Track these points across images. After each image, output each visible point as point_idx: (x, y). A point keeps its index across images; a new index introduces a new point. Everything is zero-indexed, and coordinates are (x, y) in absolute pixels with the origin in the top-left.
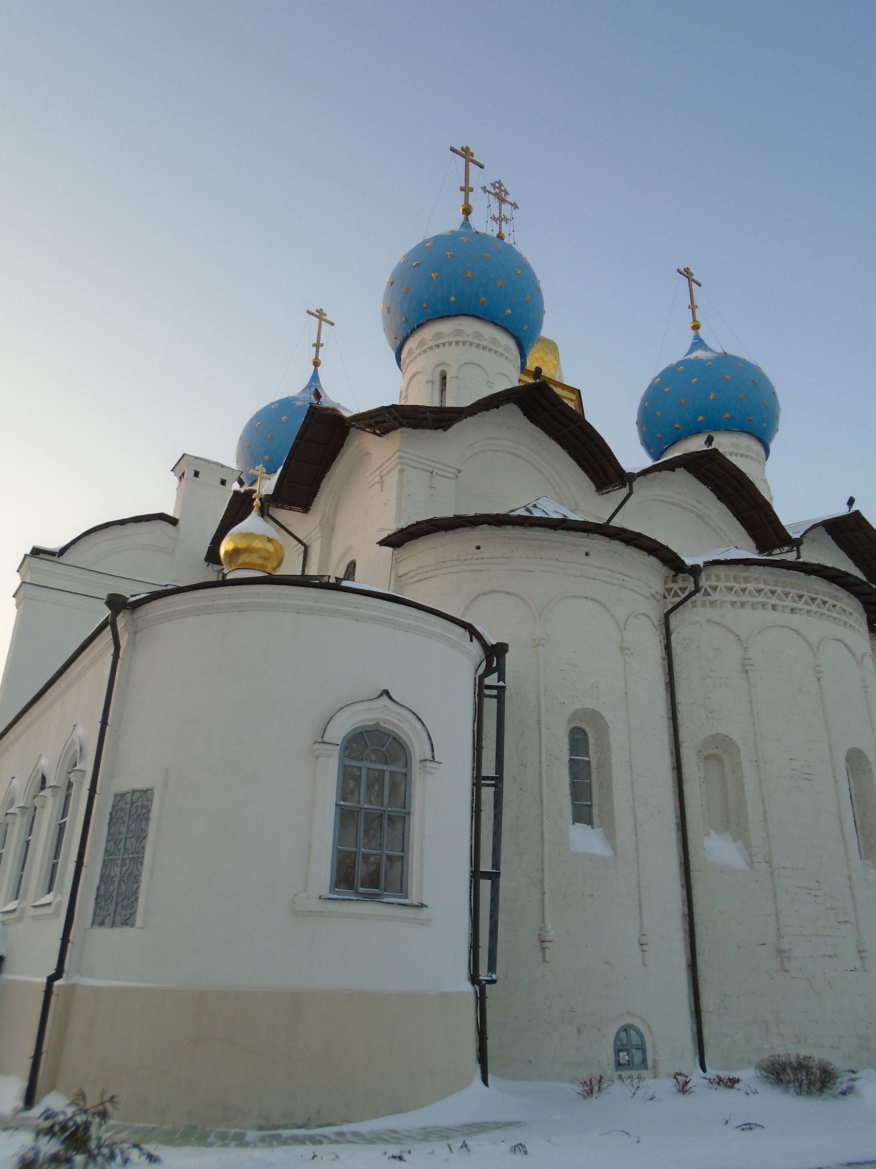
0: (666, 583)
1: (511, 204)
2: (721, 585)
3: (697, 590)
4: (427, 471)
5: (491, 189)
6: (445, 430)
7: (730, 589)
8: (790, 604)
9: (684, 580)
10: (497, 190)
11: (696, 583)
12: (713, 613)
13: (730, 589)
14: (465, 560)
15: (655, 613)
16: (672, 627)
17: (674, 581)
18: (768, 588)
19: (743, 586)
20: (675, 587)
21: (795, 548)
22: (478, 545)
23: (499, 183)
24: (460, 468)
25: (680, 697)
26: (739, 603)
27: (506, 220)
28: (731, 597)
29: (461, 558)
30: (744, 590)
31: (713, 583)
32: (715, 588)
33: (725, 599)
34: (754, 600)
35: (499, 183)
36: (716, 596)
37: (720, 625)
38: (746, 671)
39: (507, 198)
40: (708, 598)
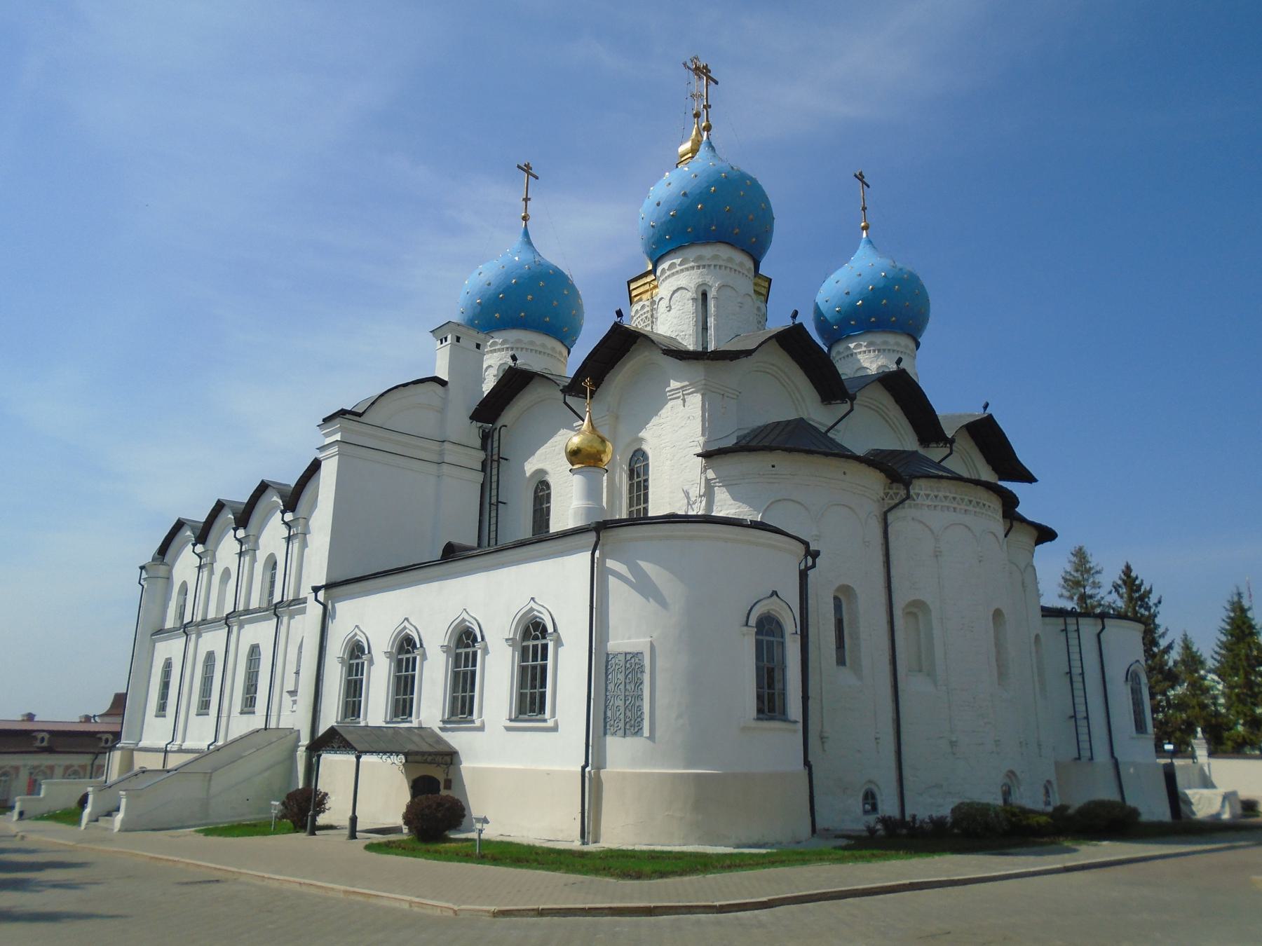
0: (885, 489)
2: (922, 493)
3: (908, 497)
4: (720, 394)
8: (964, 507)
9: (897, 489)
11: (908, 492)
13: (928, 496)
14: (763, 475)
16: (889, 521)
17: (889, 488)
18: (951, 495)
19: (936, 493)
20: (891, 492)
21: (948, 445)
22: (773, 464)
26: (933, 506)
28: (928, 502)
29: (761, 473)
31: (917, 491)
32: (918, 495)
33: (924, 503)
34: (943, 504)
36: (919, 501)
37: (921, 522)
38: (937, 556)
40: (915, 502)
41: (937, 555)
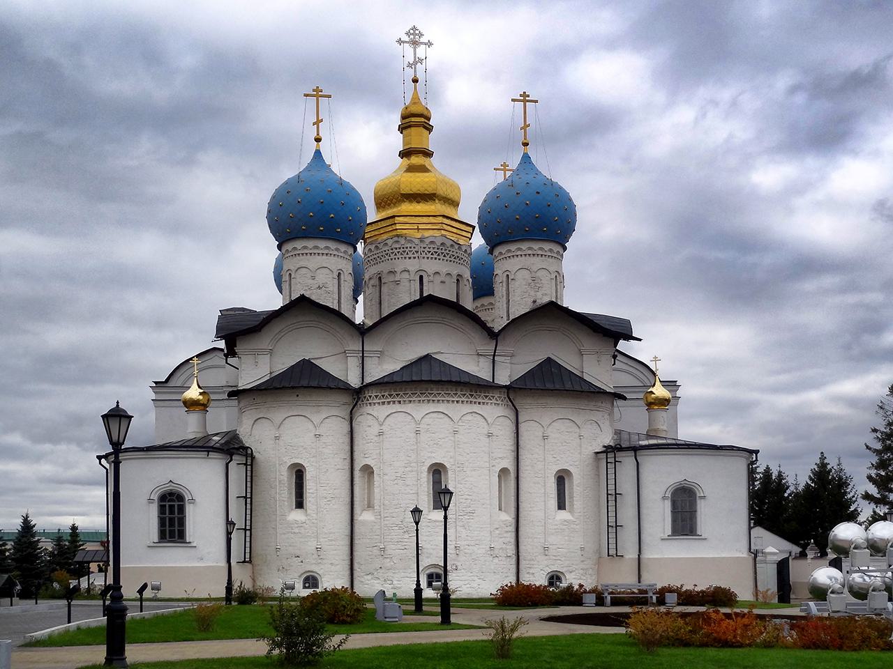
1: (426, 44)
5: (407, 39)
6: (260, 331)
7: (376, 396)
10: (412, 37)
12: (369, 409)
13: (376, 396)
15: (346, 414)
23: (414, 28)
24: (271, 348)
25: (356, 448)
27: (421, 61)
30: (383, 396)
32: (370, 397)
35: (414, 28)
39: (422, 40)
41: (381, 434)
